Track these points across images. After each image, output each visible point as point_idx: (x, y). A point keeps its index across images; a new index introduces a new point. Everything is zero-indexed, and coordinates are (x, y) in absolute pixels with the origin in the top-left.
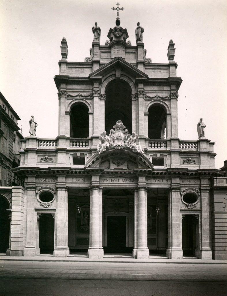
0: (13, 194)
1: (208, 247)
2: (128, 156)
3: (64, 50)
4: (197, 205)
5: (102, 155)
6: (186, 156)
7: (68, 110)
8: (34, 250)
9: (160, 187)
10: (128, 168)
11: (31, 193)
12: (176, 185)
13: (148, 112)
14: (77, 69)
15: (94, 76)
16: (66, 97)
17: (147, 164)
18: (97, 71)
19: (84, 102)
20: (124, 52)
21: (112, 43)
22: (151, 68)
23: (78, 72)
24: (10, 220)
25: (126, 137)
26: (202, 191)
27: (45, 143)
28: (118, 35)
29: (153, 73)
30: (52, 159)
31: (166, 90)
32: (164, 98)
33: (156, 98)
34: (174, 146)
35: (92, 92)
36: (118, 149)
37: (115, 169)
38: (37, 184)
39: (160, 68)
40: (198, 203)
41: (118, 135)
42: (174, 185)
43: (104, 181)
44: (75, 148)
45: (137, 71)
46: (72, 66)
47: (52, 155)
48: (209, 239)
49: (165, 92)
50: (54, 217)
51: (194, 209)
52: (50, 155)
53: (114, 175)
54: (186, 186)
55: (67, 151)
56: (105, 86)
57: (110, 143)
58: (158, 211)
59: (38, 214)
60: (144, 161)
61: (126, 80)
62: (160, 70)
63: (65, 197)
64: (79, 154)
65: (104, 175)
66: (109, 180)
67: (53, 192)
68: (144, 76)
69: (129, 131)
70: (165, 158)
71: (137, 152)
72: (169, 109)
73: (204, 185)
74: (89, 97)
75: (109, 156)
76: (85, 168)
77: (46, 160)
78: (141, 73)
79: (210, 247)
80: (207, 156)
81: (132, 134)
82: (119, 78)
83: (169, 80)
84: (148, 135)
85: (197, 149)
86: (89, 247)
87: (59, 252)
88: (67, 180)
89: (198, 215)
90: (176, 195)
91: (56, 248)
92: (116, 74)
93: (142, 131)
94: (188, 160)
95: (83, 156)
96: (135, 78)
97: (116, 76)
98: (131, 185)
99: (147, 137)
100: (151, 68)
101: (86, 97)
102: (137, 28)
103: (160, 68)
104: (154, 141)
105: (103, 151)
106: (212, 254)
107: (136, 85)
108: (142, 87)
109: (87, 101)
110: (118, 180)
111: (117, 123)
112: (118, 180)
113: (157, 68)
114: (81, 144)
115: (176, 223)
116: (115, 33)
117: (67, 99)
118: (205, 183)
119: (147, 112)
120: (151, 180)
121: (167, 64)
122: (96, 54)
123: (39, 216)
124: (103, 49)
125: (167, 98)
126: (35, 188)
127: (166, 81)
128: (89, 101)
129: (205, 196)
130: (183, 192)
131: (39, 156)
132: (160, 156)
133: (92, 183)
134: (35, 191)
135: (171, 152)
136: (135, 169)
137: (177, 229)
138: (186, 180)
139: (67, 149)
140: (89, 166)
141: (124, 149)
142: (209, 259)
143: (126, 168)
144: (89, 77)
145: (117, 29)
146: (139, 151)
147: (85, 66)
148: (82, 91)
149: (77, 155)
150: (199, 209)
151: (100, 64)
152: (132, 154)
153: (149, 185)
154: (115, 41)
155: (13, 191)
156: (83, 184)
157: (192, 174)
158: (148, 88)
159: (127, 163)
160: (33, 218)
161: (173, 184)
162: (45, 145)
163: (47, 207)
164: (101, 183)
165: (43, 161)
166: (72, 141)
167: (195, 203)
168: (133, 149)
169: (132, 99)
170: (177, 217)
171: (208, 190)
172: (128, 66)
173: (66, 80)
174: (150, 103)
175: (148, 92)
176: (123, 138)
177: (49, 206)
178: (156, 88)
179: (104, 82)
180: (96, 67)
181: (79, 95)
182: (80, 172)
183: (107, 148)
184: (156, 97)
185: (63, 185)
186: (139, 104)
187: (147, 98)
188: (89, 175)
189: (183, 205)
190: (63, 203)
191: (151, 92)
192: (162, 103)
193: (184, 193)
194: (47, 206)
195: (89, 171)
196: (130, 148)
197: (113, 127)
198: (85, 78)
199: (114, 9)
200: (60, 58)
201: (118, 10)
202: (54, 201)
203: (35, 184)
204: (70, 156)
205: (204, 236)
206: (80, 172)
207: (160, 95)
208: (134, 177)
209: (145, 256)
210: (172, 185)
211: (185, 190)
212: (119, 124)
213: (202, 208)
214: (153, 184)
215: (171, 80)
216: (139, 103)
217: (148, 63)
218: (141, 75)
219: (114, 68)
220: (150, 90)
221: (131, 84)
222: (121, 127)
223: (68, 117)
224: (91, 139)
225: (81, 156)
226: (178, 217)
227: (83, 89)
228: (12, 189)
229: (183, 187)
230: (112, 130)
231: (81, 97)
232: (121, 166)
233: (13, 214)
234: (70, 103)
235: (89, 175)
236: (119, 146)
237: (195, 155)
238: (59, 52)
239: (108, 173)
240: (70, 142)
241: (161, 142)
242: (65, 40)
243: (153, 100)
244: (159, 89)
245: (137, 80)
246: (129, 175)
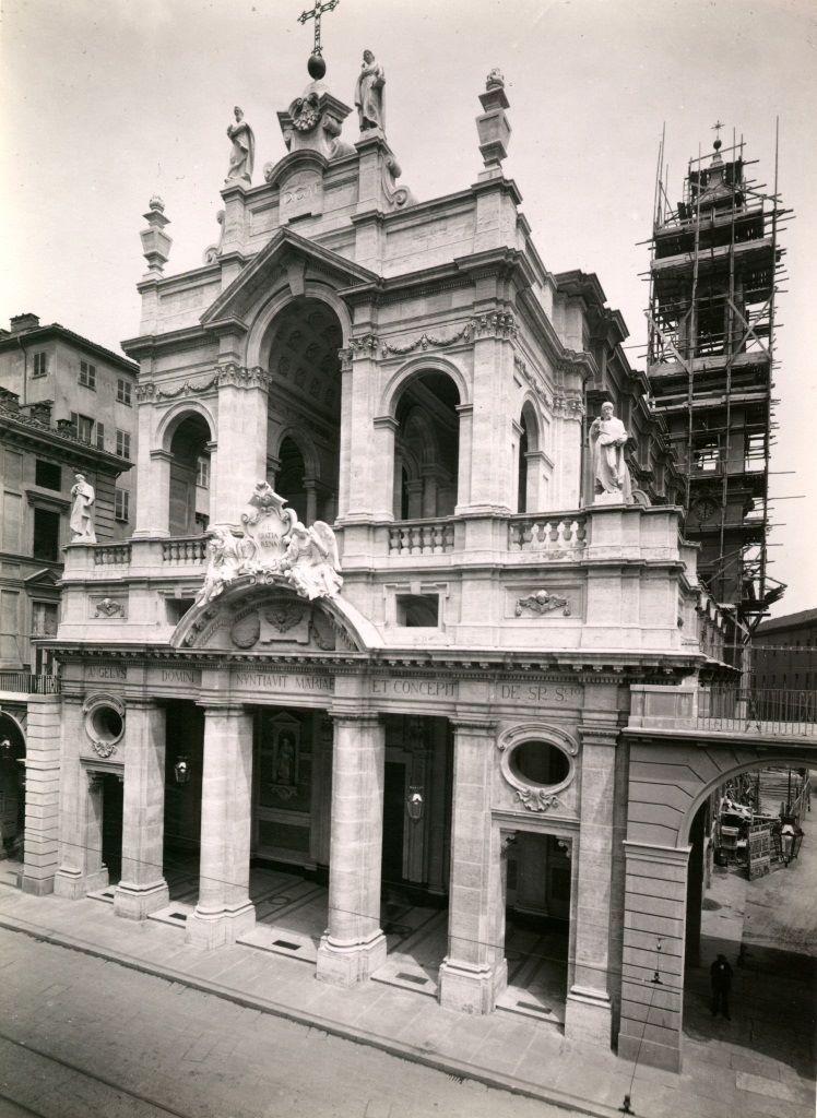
0: (30, 719)
1: (597, 987)
3: (150, 243)
4: (565, 795)
6: (529, 584)
7: (386, 411)
8: (73, 881)
9: (417, 712)
11: (73, 715)
12: (474, 709)
14: (185, 294)
16: (155, 401)
19: (441, 367)
20: (318, 190)
22: (409, 223)
23: (187, 305)
24: (23, 791)
26: (586, 740)
27: (548, 528)
28: (306, 127)
30: (564, 604)
31: (463, 304)
32: (448, 343)
33: (419, 350)
34: (473, 547)
37: (273, 641)
38: (86, 685)
39: (441, 214)
40: (568, 787)
42: (466, 708)
45: (343, 264)
46: (171, 291)
47: (119, 593)
48: (606, 954)
49: (453, 316)
50: (568, 854)
51: (551, 814)
52: (116, 594)
53: (267, 666)
54: (542, 712)
55: (150, 584)
56: (261, 336)
59: (503, 832)
62: (442, 224)
63: (142, 730)
64: (416, 588)
66: (442, 691)
67: (569, 751)
70: (442, 595)
72: (465, 386)
73: (596, 716)
77: (539, 607)
79: (608, 990)
80: (618, 581)
82: (302, 296)
85: (581, 551)
86: (575, 988)
87: (124, 900)
88: (151, 675)
89: (569, 841)
90: (472, 753)
91: (574, 993)
93: (358, 496)
94: (537, 600)
95: (431, 592)
98: (320, 699)
100: (409, 223)
101: (444, 346)
102: (365, 75)
103: (441, 214)
104: (408, 526)
106: (609, 1024)
108: (367, 319)
109: (448, 358)
110: (282, 679)
112: (282, 679)
113: (427, 219)
114: (427, 540)
115: (468, 865)
117: (158, 406)
118: (599, 704)
119: (386, 413)
120: (387, 684)
121: (468, 191)
123: (508, 840)
124: (258, 198)
126: (491, 729)
127: (451, 273)
128: (457, 361)
129: (595, 768)
130: (510, 737)
131: (510, 589)
132: (422, 588)
134: (495, 738)
135: (459, 573)
137: (472, 889)
138: (525, 687)
142: (597, 1042)
145: (302, 106)
147: (204, 281)
148: (193, 371)
149: (409, 589)
150: (571, 817)
153: (381, 703)
154: (289, 161)
155: (30, 708)
156: (187, 691)
157: (535, 667)
158: (386, 316)
160: (77, 784)
161: (462, 704)
162: (548, 538)
163: (540, 810)
164: (233, 691)
165: (526, 614)
166: (393, 532)
167: (557, 788)
169: (343, 369)
170: (471, 842)
171: (611, 736)
172: (313, 253)
173: (150, 347)
175: (390, 330)
177: (551, 809)
178: (420, 307)
179: (256, 319)
180: (230, 276)
181: (186, 387)
184: (418, 344)
185: (137, 693)
186: (355, 388)
187: (389, 356)
189: (505, 792)
190: (137, 749)
191: (403, 327)
193: (514, 740)
194: (541, 807)
198: (194, 329)
200: (141, 270)
202: (568, 787)
203: (79, 685)
204: (385, 595)
205: (589, 937)
207: (436, 335)
208: (323, 672)
209: (339, 976)
210: (585, 715)
211: (518, 732)
213: (583, 813)
214: (393, 700)
215: (467, 266)
216: (355, 383)
218: (356, 275)
219: (279, 266)
220: (399, 323)
221: (340, 310)
223: (387, 437)
224: (464, 521)
225: (186, 597)
226: (477, 842)
227: (196, 366)
228: (26, 702)
229: (508, 717)
232: (290, 631)
233: (29, 774)
234: (163, 420)
237: (571, 575)
238: (139, 250)
240: (391, 536)
241: (414, 529)
242: (499, 83)
243: (408, 360)
244: (433, 310)
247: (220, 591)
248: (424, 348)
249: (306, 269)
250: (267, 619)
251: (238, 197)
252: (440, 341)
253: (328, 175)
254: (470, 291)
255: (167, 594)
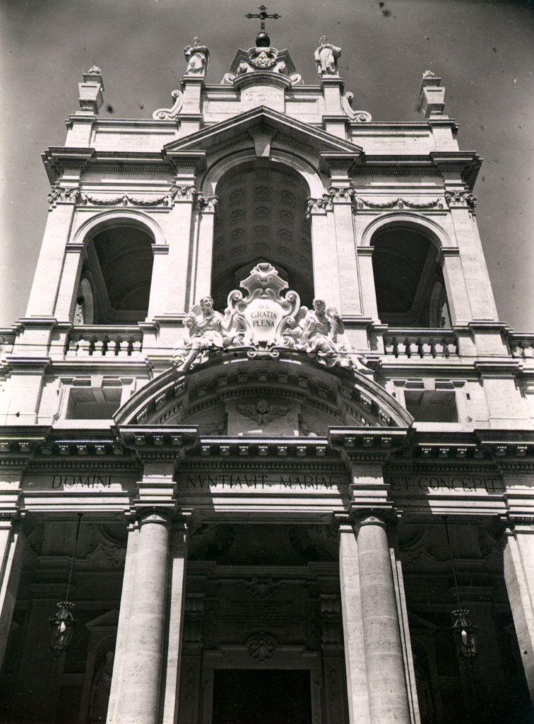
2: (303, 384)
5: (191, 377)
10: (305, 432)
13: (371, 245)
15: (181, 149)
17: (384, 411)
18: (191, 138)
21: (245, 78)
25: (292, 318)
29: (378, 145)
35: (171, 190)
36: (257, 358)
39: (399, 133)
41: (259, 310)
43: (198, 484)
44: (80, 355)
57: (224, 336)
58: (464, 633)
60: (372, 401)
61: (287, 164)
65: (196, 459)
68: (346, 149)
69: (299, 294)
70: (459, 393)
71: (338, 364)
74: (159, 206)
75: (225, 383)
76: (115, 429)
78: (337, 142)
81: (314, 304)
83: (435, 159)
84: (377, 316)
92: (254, 148)
96: (317, 155)
97: (254, 153)
99: (377, 321)
105: (197, 361)
107: (324, 173)
111: (254, 272)
116: (253, 60)
119: (367, 243)
122: (193, 101)
125: (437, 208)
132: (437, 386)
133: (142, 491)
136: (332, 432)
139: (52, 362)
140: (134, 421)
141: (282, 356)
143: (296, 433)
144: (164, 152)
146: (344, 363)
151: (202, 125)
152: (318, 376)
159: (298, 411)
168: (321, 354)
169: (313, 211)
174: (376, 220)
176: (278, 321)
179: (213, 166)
180: (189, 129)
182: (91, 449)
183: (211, 350)
188: (133, 458)
192: (419, 221)
195: (131, 439)
196: (309, 350)
197: (241, 285)
199: (250, 16)
201: (264, 42)
206: (91, 449)
212: (263, 275)
217: (360, 121)
222: (273, 285)
230: (236, 293)
231: (130, 205)
235: (133, 458)
236: (263, 344)
239: (215, 449)
245: (322, 160)
246: (307, 460)
247: (205, 360)
248: (401, 205)
249: (272, 140)
250: (238, 410)
251: (200, 85)
252: (415, 203)
253: (289, 93)
254: (438, 179)
255: (76, 383)
